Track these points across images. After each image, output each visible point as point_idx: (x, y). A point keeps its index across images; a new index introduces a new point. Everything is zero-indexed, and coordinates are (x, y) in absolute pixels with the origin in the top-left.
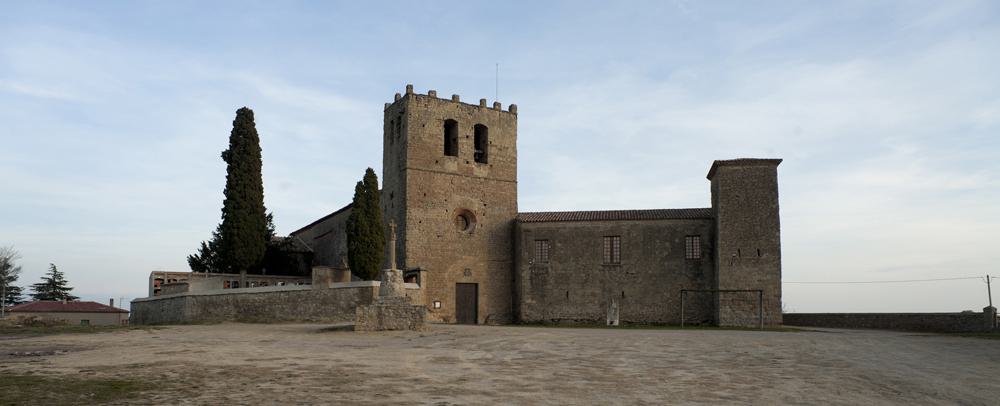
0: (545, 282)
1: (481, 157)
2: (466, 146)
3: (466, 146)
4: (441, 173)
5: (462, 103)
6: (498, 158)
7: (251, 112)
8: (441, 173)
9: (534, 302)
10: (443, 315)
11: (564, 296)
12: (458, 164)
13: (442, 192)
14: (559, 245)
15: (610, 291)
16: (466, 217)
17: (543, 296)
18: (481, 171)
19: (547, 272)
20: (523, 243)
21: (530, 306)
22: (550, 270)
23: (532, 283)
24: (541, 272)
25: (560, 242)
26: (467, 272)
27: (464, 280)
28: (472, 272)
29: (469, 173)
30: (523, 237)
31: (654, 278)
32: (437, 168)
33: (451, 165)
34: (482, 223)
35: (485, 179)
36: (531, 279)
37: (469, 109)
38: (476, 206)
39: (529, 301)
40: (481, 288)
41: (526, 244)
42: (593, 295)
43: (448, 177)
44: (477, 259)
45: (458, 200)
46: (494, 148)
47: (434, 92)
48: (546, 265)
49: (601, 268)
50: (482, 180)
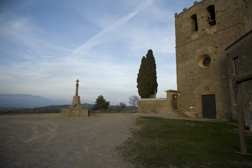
1: (212, 23)
2: (202, 22)
3: (202, 22)
4: (190, 42)
6: (223, 16)
7: (151, 50)
8: (190, 42)
10: (195, 113)
12: (198, 34)
13: (191, 51)
16: (207, 60)
18: (214, 29)
26: (207, 88)
27: (206, 93)
28: (210, 88)
29: (206, 35)
32: (189, 40)
33: (195, 36)
34: (215, 59)
35: (214, 33)
37: (202, 3)
38: (210, 50)
40: (217, 97)
41: (229, 64)
43: (194, 42)
44: (213, 80)
45: (199, 51)
46: (220, 13)
47: (186, 8)
50: (214, 35)
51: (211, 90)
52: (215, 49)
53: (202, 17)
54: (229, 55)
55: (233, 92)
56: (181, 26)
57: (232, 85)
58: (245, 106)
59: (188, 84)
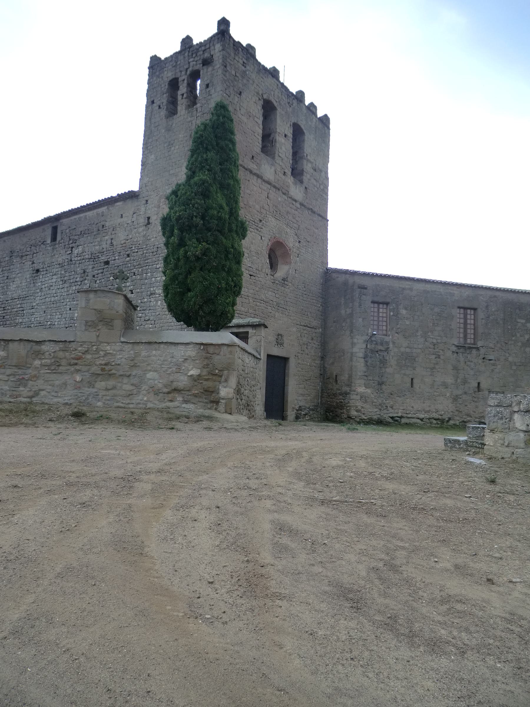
0: (383, 362)
5: (282, 84)
9: (369, 391)
11: (409, 385)
14: (404, 312)
15: (465, 382)
17: (381, 384)
19: (387, 350)
20: (357, 304)
21: (364, 398)
22: (391, 345)
23: (366, 362)
24: (380, 347)
25: (406, 309)
30: (357, 294)
31: (514, 368)
36: (365, 357)
39: (361, 389)
40: (292, 367)
41: (360, 305)
42: (445, 385)
48: (387, 339)
49: (454, 349)
50: (299, 206)
51: (285, 345)
52: (297, 244)
53: (285, 136)
54: (365, 290)
55: (363, 365)
56: (240, 94)
57: (363, 350)
58: (392, 394)
59: (243, 309)
